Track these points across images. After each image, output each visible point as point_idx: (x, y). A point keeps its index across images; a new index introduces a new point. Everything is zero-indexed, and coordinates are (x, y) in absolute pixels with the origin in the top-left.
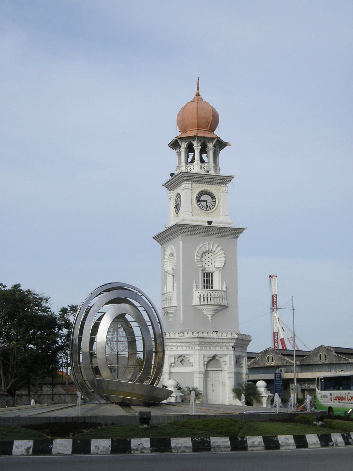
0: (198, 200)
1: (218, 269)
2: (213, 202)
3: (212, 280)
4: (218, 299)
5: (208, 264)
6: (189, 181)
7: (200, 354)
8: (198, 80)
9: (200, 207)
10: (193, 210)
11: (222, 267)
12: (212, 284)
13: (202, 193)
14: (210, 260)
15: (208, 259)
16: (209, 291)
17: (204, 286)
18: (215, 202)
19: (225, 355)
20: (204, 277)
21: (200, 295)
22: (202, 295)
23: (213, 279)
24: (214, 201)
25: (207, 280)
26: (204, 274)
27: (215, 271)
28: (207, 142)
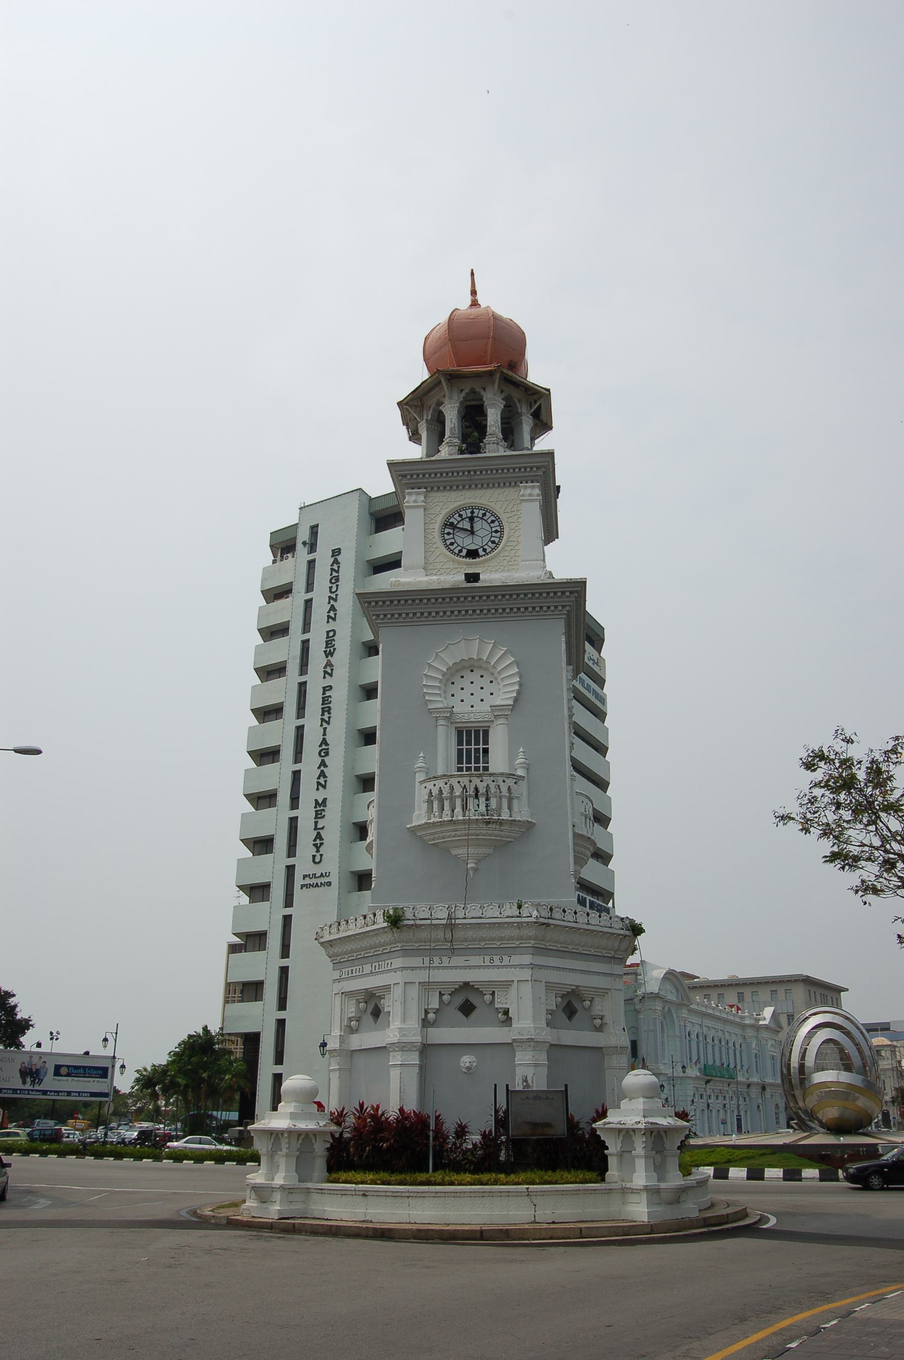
3: (486, 751)
5: (469, 700)
7: (405, 983)
9: (452, 551)
10: (431, 560)
11: (511, 702)
15: (469, 688)
19: (506, 985)
20: (460, 742)
21: (431, 793)
22: (435, 792)
23: (491, 747)
25: (469, 752)
26: (460, 733)
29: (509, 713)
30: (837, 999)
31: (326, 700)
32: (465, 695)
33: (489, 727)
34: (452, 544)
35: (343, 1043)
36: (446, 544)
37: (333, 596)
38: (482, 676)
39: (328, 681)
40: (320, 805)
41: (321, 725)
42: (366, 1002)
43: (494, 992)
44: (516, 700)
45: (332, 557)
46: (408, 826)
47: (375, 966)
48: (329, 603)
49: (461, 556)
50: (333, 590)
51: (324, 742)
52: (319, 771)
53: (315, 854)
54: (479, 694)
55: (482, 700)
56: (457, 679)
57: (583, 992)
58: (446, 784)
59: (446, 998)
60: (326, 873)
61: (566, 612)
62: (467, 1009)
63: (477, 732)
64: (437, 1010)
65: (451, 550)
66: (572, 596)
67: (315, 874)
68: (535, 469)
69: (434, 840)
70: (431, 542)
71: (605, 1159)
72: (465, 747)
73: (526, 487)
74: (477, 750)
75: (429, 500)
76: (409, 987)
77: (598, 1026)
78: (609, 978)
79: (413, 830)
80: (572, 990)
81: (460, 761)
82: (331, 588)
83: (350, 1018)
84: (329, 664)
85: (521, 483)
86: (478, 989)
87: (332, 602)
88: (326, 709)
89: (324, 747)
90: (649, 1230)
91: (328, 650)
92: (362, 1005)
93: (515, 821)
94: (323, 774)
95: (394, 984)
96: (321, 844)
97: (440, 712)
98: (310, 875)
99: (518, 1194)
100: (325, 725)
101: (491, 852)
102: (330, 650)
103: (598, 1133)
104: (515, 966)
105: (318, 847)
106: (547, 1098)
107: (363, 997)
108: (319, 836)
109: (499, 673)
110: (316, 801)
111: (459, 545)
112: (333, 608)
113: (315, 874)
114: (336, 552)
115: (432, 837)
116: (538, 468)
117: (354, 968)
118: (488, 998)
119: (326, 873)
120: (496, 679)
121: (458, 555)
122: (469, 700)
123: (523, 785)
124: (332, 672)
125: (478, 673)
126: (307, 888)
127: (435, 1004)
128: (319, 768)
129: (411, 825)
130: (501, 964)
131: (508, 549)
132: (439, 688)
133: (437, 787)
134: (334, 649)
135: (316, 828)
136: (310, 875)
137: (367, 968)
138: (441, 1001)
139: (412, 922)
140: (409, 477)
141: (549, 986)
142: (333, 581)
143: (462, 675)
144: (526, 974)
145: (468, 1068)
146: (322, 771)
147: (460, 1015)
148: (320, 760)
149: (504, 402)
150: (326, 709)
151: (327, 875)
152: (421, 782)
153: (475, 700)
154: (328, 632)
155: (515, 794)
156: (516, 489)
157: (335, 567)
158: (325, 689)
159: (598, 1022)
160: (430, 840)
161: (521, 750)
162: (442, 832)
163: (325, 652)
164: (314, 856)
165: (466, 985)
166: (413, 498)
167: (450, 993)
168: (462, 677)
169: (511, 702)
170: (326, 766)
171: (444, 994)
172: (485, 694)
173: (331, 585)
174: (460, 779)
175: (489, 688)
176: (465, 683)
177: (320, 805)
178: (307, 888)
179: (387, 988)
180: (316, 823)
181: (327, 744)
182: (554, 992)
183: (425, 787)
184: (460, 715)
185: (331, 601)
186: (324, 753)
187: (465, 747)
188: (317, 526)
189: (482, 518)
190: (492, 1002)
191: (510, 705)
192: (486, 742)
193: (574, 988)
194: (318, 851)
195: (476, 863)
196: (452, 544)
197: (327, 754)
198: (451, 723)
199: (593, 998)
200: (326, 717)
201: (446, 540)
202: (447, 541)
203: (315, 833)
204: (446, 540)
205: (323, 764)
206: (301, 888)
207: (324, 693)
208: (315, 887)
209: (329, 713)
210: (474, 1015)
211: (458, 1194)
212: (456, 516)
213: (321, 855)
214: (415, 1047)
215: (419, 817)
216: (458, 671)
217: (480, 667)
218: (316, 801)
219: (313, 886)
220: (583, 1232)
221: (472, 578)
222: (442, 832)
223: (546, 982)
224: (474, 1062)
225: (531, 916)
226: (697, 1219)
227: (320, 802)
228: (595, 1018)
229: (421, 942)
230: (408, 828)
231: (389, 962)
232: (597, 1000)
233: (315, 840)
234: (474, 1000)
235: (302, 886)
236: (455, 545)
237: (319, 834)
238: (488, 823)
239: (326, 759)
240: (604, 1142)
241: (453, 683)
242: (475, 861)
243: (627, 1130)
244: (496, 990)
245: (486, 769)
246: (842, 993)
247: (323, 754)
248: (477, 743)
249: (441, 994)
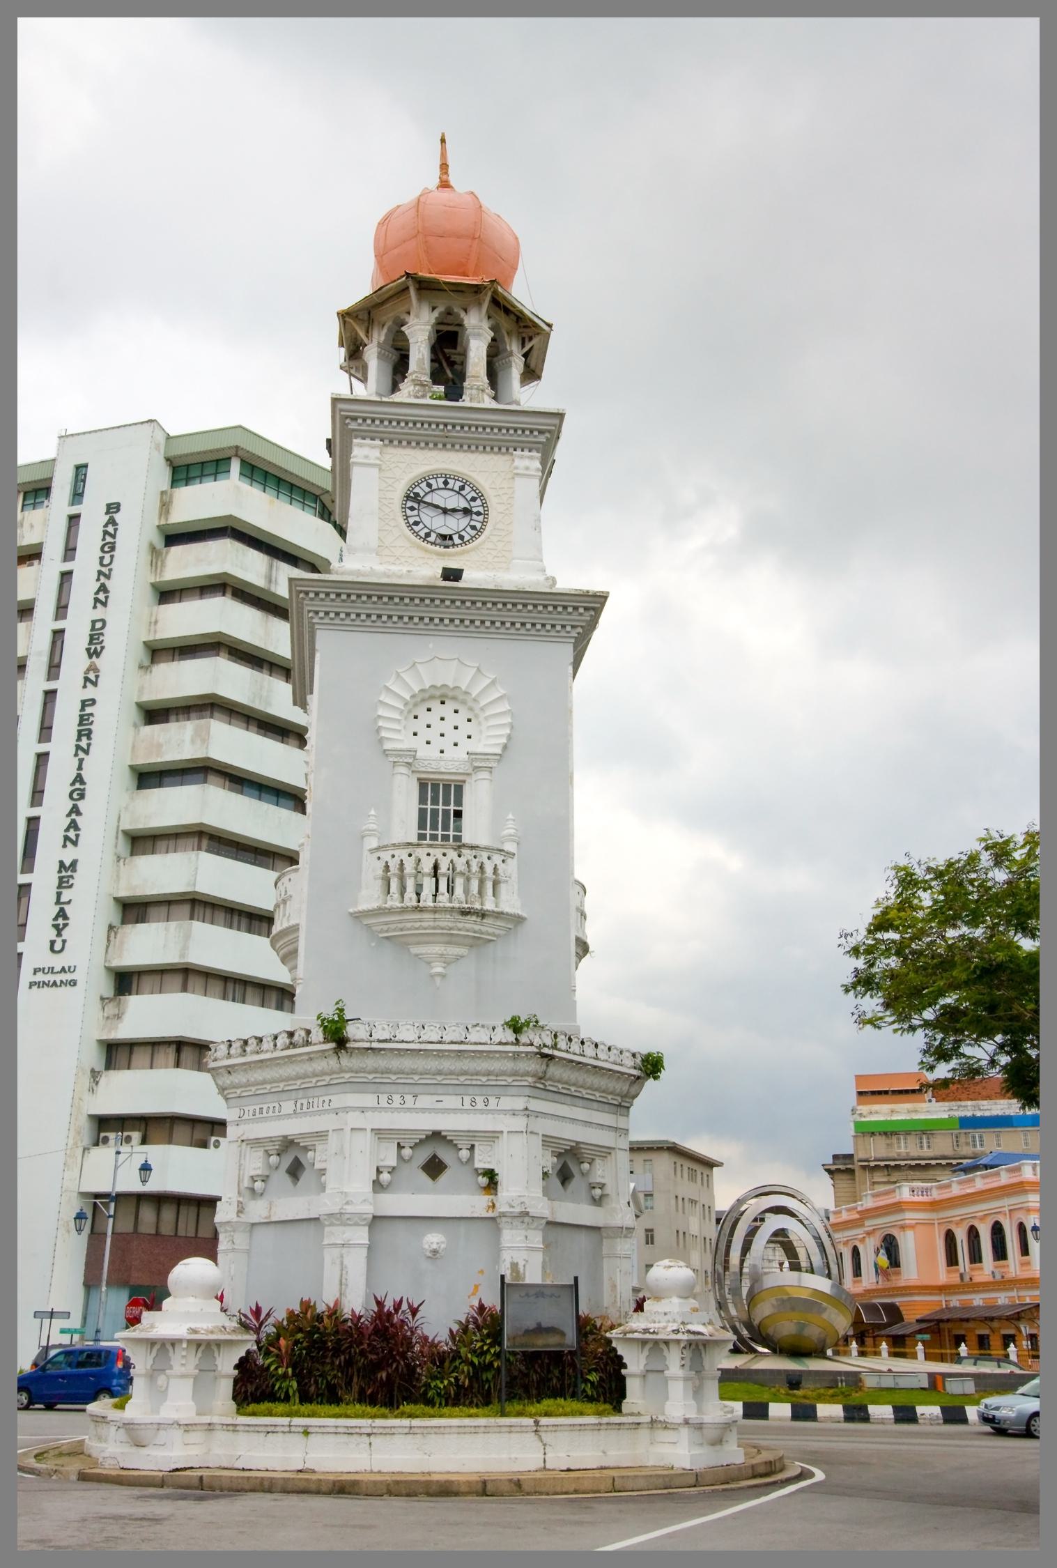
1: (479, 763)
3: (458, 814)
5: (438, 743)
6: (373, 439)
7: (352, 1129)
8: (443, 141)
15: (438, 727)
20: (422, 800)
21: (387, 867)
23: (466, 809)
26: (423, 785)
27: (468, 774)
28: (462, 314)
29: (494, 765)
30: (708, 1176)
31: (84, 719)
32: (432, 734)
33: (464, 781)
34: (416, 523)
35: (242, 1212)
36: (408, 522)
37: (105, 570)
38: (456, 711)
39: (90, 692)
40: (67, 871)
41: (76, 755)
42: (278, 1155)
43: (473, 1146)
44: (505, 747)
45: (106, 513)
46: (351, 910)
47: (302, 1104)
48: (98, 580)
49: (428, 542)
50: (106, 561)
51: (79, 779)
52: (69, 820)
53: (54, 938)
54: (452, 736)
55: (456, 745)
56: (421, 711)
57: (583, 1151)
58: (410, 855)
59: (407, 1152)
60: (70, 967)
61: (576, 635)
62: (434, 1168)
63: (447, 787)
64: (394, 1168)
65: (415, 532)
66: (587, 614)
67: (53, 968)
68: (536, 433)
69: (387, 931)
70: (387, 517)
71: (622, 1381)
72: (429, 807)
73: (522, 457)
74: (446, 813)
75: (387, 457)
76: (359, 1135)
77: (597, 1197)
78: (614, 1133)
79: (358, 916)
80: (571, 1146)
81: (422, 825)
82: (102, 559)
83: (252, 1177)
84: (93, 668)
85: (515, 450)
86: (452, 1141)
87: (103, 579)
88: (85, 730)
89: (78, 786)
90: (692, 1481)
91: (93, 647)
92: (274, 1159)
93: (502, 913)
94: (74, 825)
95: (333, 1130)
96: (65, 925)
97: (399, 755)
98: (44, 969)
99: (523, 1429)
100: (81, 755)
101: (465, 954)
102: (96, 648)
103: (614, 1345)
104: (505, 1112)
105: (59, 930)
106: (552, 1295)
107: (277, 1147)
108: (62, 914)
109: (482, 709)
110: (62, 864)
111: (426, 527)
112: (103, 588)
113: (53, 968)
114: (113, 508)
115: (385, 928)
116: (541, 432)
117: (265, 1107)
118: (464, 1154)
119: (70, 967)
120: (476, 716)
121: (424, 540)
122: (438, 743)
123: (512, 864)
124: (97, 680)
125: (450, 706)
126: (39, 987)
127: (392, 1161)
128: (69, 815)
129: (356, 910)
130: (485, 1108)
131: (494, 539)
132: (398, 721)
133: (397, 860)
134: (103, 648)
135: (58, 902)
136: (44, 969)
137: (288, 1107)
138: (400, 1157)
139: (367, 1045)
140: (360, 421)
141: (547, 1141)
142: (106, 549)
143: (429, 707)
144: (519, 1123)
145: (435, 1252)
146: (73, 821)
147: (424, 1177)
148: (70, 804)
149: (492, 334)
150: (85, 730)
151: (71, 970)
152: (373, 851)
153: (446, 743)
154: (94, 622)
156: (507, 457)
157: (110, 529)
158: (84, 704)
159: (598, 1192)
160: (382, 931)
161: (510, 816)
162: (400, 922)
163: (88, 650)
164: (53, 943)
165: (436, 1136)
166: (366, 451)
167: (412, 1145)
168: (429, 710)
169: (498, 751)
170: (78, 813)
171: (404, 1147)
172: (460, 736)
173: (102, 555)
174: (431, 851)
175: (466, 728)
176: (433, 718)
177: (67, 871)
178: (39, 987)
179: (322, 1135)
180: (59, 895)
181: (82, 782)
182: (551, 1149)
183: (379, 858)
184: (426, 763)
185: (102, 578)
186: (78, 794)
187: (429, 807)
188: (86, 466)
189: (459, 493)
190: (471, 1159)
191: (496, 754)
192: (459, 801)
193: (574, 1144)
194: (59, 935)
195: (444, 968)
196: (416, 523)
197: (82, 796)
198: (413, 772)
199: (593, 1159)
200: (84, 743)
201: (407, 517)
202: (409, 519)
203: (57, 909)
204: (407, 517)
205: (75, 810)
206: (30, 987)
207: (83, 709)
208: (52, 986)
209: (89, 738)
210: (444, 1178)
211: (442, 1429)
212: (424, 485)
213: (64, 942)
214: (365, 1219)
215: (370, 897)
216: (423, 700)
217: (454, 698)
218: (62, 864)
219: (48, 985)
220: (616, 1483)
221: (452, 575)
222: (400, 922)
223: (543, 1135)
224: (442, 1243)
225: (532, 1045)
226: (740, 1468)
227: (67, 864)
228: (594, 1188)
229: (376, 1073)
230: (351, 914)
231: (327, 1099)
232: (598, 1161)
233: (56, 919)
234: (445, 1155)
235: (31, 985)
236: (421, 526)
237: (62, 910)
238: (465, 913)
239: (81, 804)
240: (620, 1358)
241: (416, 717)
242: (444, 965)
243: (656, 1342)
244: (476, 1144)
245: (458, 839)
246: (715, 1169)
247: (75, 796)
248: (446, 803)
249: (400, 1147)
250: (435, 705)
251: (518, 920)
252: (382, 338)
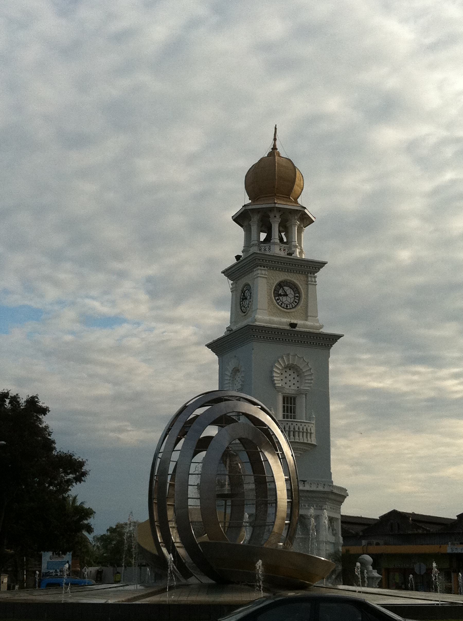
0: (277, 295)
2: (296, 298)
3: (295, 407)
4: (305, 434)
12: (294, 413)
13: (280, 285)
14: (292, 379)
15: (289, 378)
16: (291, 423)
17: (284, 415)
18: (299, 297)
24: (297, 297)
25: (287, 407)
33: (296, 397)
63: (291, 398)
155: (312, 431)
187: (286, 405)
236: (279, 301)
250: (288, 370)
251: (316, 445)
252: (258, 218)
